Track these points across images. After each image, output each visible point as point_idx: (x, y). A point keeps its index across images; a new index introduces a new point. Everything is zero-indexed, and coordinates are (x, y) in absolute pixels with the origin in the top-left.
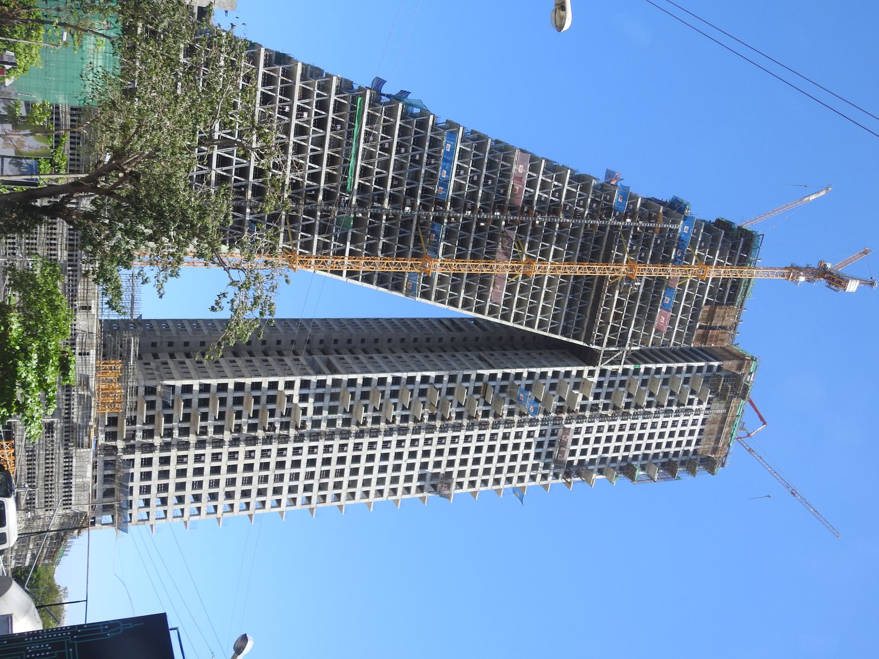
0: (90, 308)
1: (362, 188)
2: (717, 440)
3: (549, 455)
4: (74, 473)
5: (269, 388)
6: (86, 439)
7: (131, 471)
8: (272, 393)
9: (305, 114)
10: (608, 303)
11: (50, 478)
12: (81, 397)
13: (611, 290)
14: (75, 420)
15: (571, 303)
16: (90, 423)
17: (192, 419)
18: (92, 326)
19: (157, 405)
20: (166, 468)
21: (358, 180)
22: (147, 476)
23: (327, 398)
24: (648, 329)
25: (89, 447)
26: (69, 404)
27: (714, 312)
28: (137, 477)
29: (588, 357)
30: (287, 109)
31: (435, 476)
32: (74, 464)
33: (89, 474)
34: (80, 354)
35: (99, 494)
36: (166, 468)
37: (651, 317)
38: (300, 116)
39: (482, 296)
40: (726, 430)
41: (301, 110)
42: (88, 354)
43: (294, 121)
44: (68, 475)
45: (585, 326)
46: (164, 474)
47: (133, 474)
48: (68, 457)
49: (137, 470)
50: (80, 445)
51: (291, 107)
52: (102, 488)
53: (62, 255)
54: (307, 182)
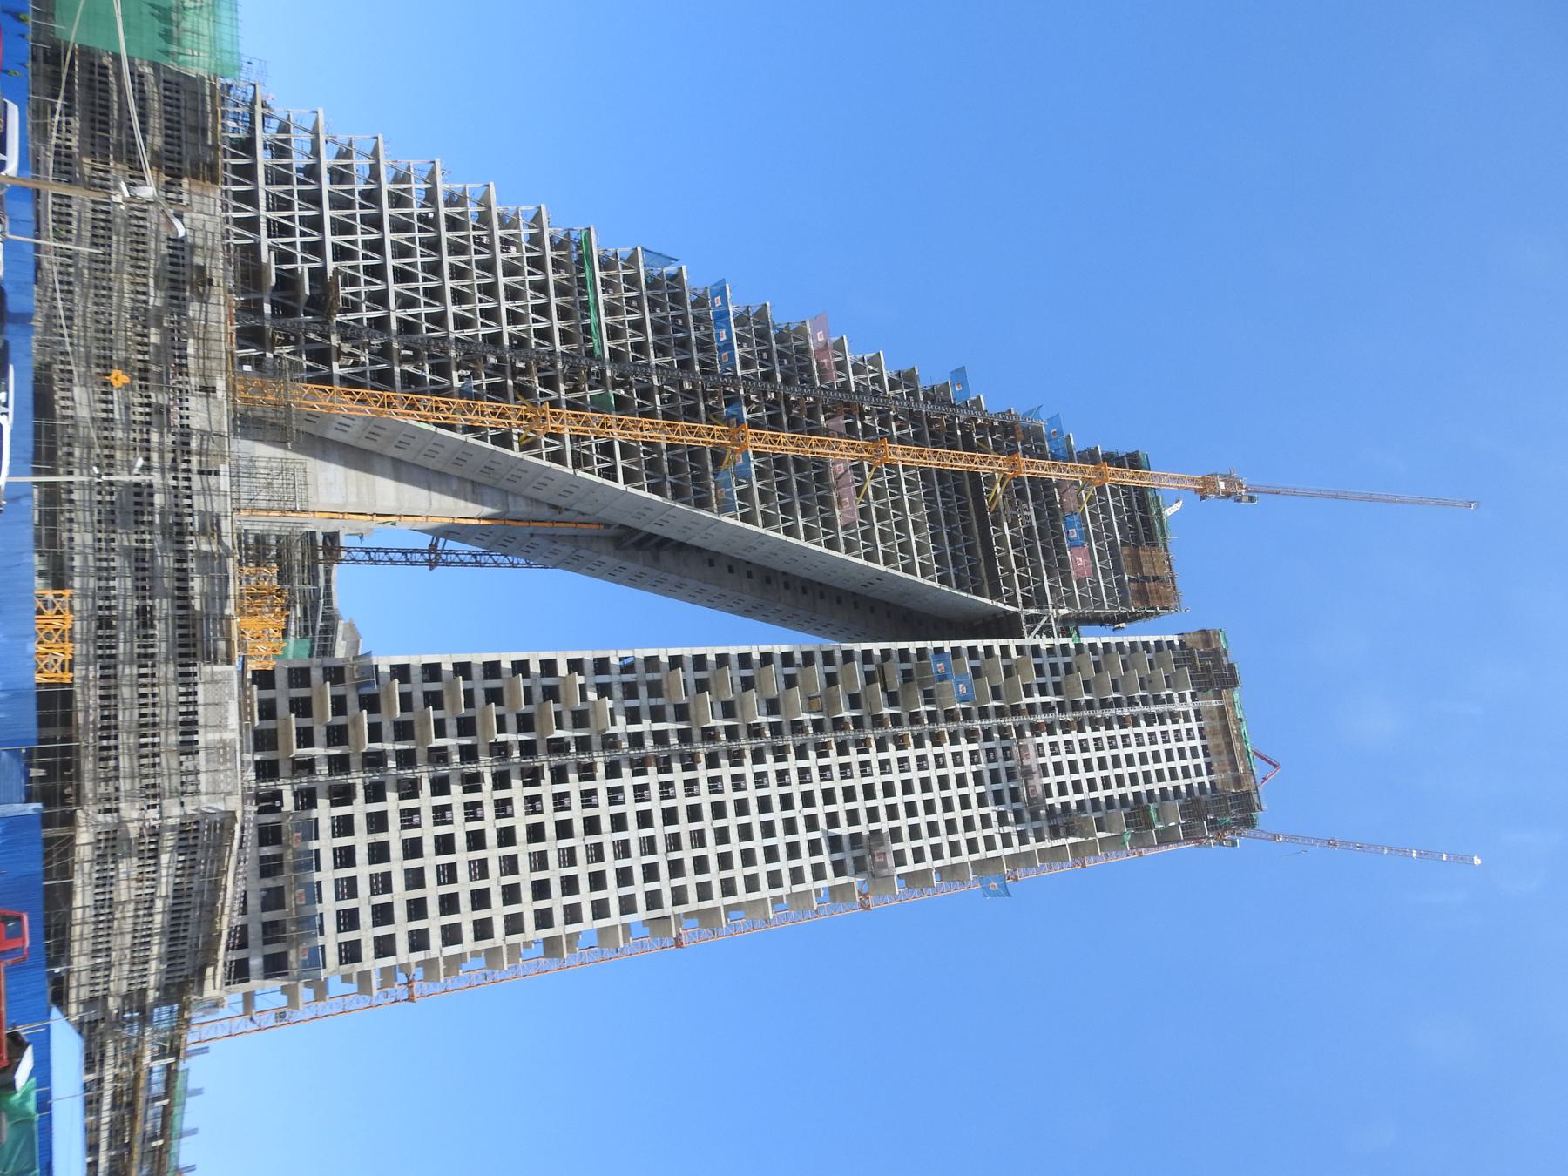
0: (214, 389)
1: (616, 355)
2: (1233, 763)
3: (1015, 795)
4: (201, 721)
5: (543, 675)
6: (222, 645)
7: (314, 845)
8: (548, 681)
9: (513, 249)
10: (1001, 541)
11: (150, 700)
12: (203, 557)
13: (997, 522)
14: (198, 607)
15: (952, 541)
16: (227, 612)
17: (417, 732)
18: (220, 423)
19: (349, 703)
20: (381, 837)
21: (607, 344)
22: (345, 857)
23: (643, 691)
24: (1067, 582)
25: (229, 662)
26: (186, 589)
27: (1138, 557)
28: (327, 859)
29: (1005, 626)
30: (486, 240)
31: (855, 839)
32: (200, 698)
33: (233, 720)
34: (201, 472)
35: (254, 902)
36: (381, 837)
37: (1063, 563)
38: (505, 250)
39: (829, 523)
40: (1236, 744)
41: (506, 243)
42: (217, 473)
43: (500, 257)
44: (189, 725)
45: (984, 574)
46: (379, 853)
47: (317, 851)
48: (186, 680)
49: (325, 844)
50: (211, 658)
51: (491, 236)
52: (255, 855)
53: (155, 300)
54: (534, 340)
